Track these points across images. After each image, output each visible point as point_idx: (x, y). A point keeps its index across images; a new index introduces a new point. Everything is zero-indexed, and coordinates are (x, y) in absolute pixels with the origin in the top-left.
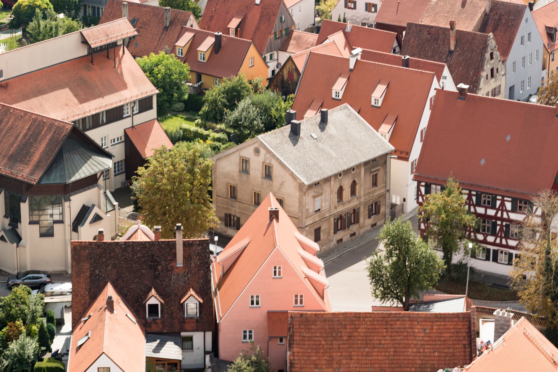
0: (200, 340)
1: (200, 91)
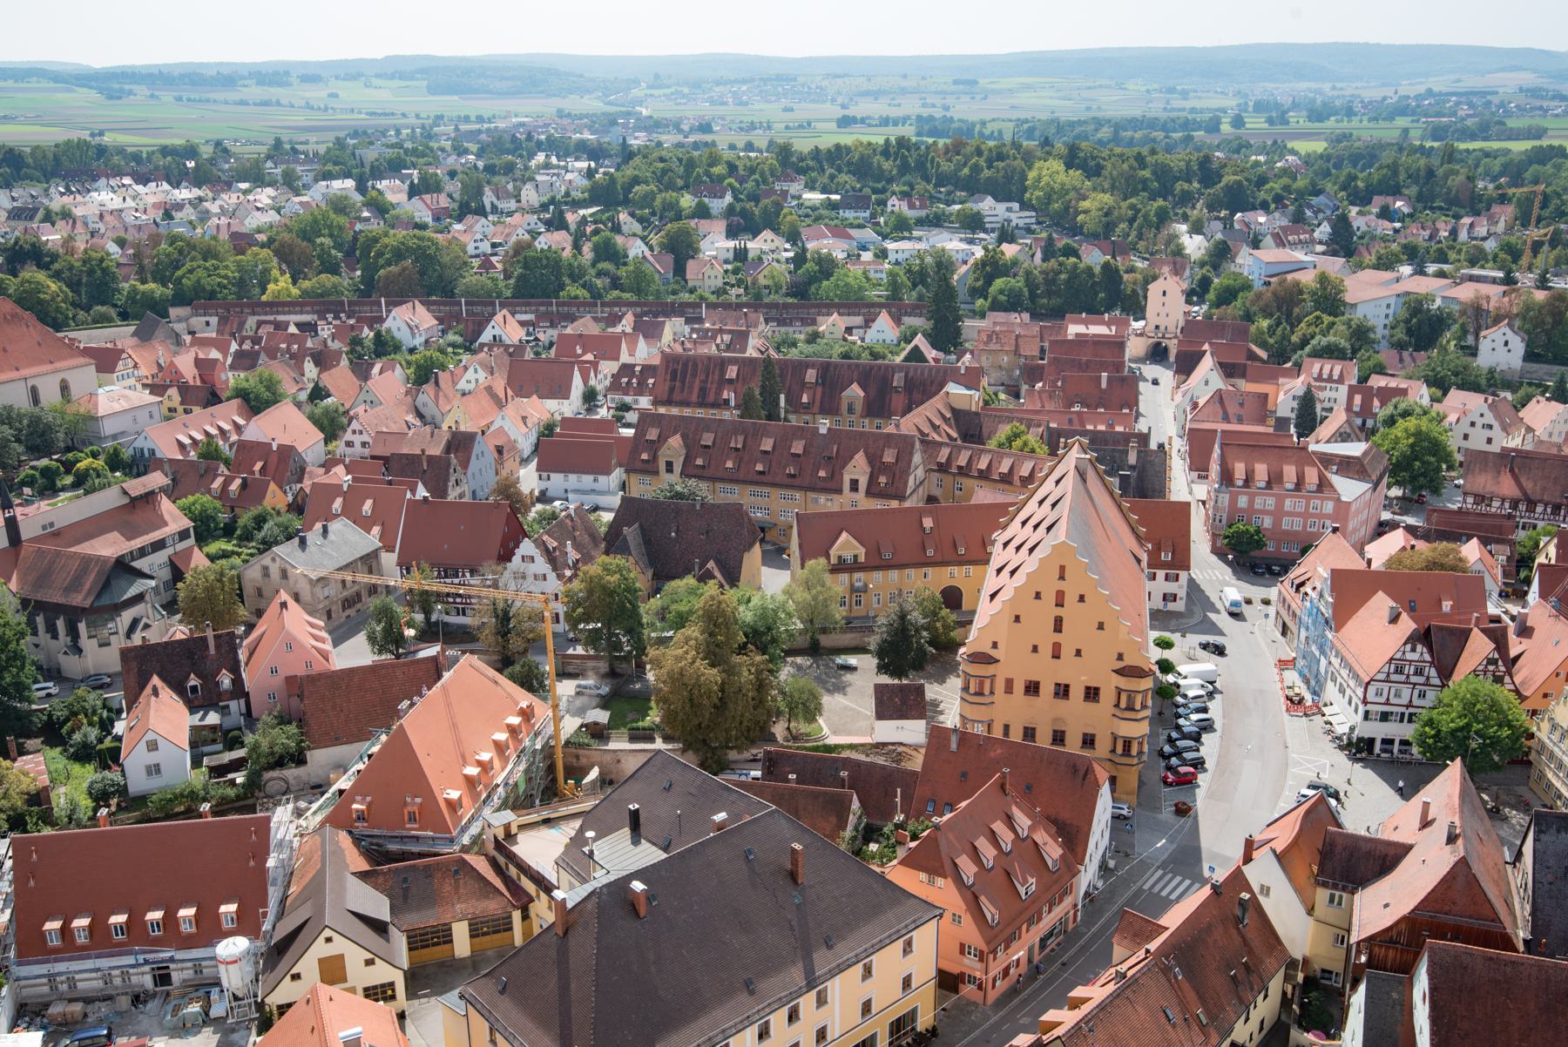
0: (235, 706)
1: (234, 520)
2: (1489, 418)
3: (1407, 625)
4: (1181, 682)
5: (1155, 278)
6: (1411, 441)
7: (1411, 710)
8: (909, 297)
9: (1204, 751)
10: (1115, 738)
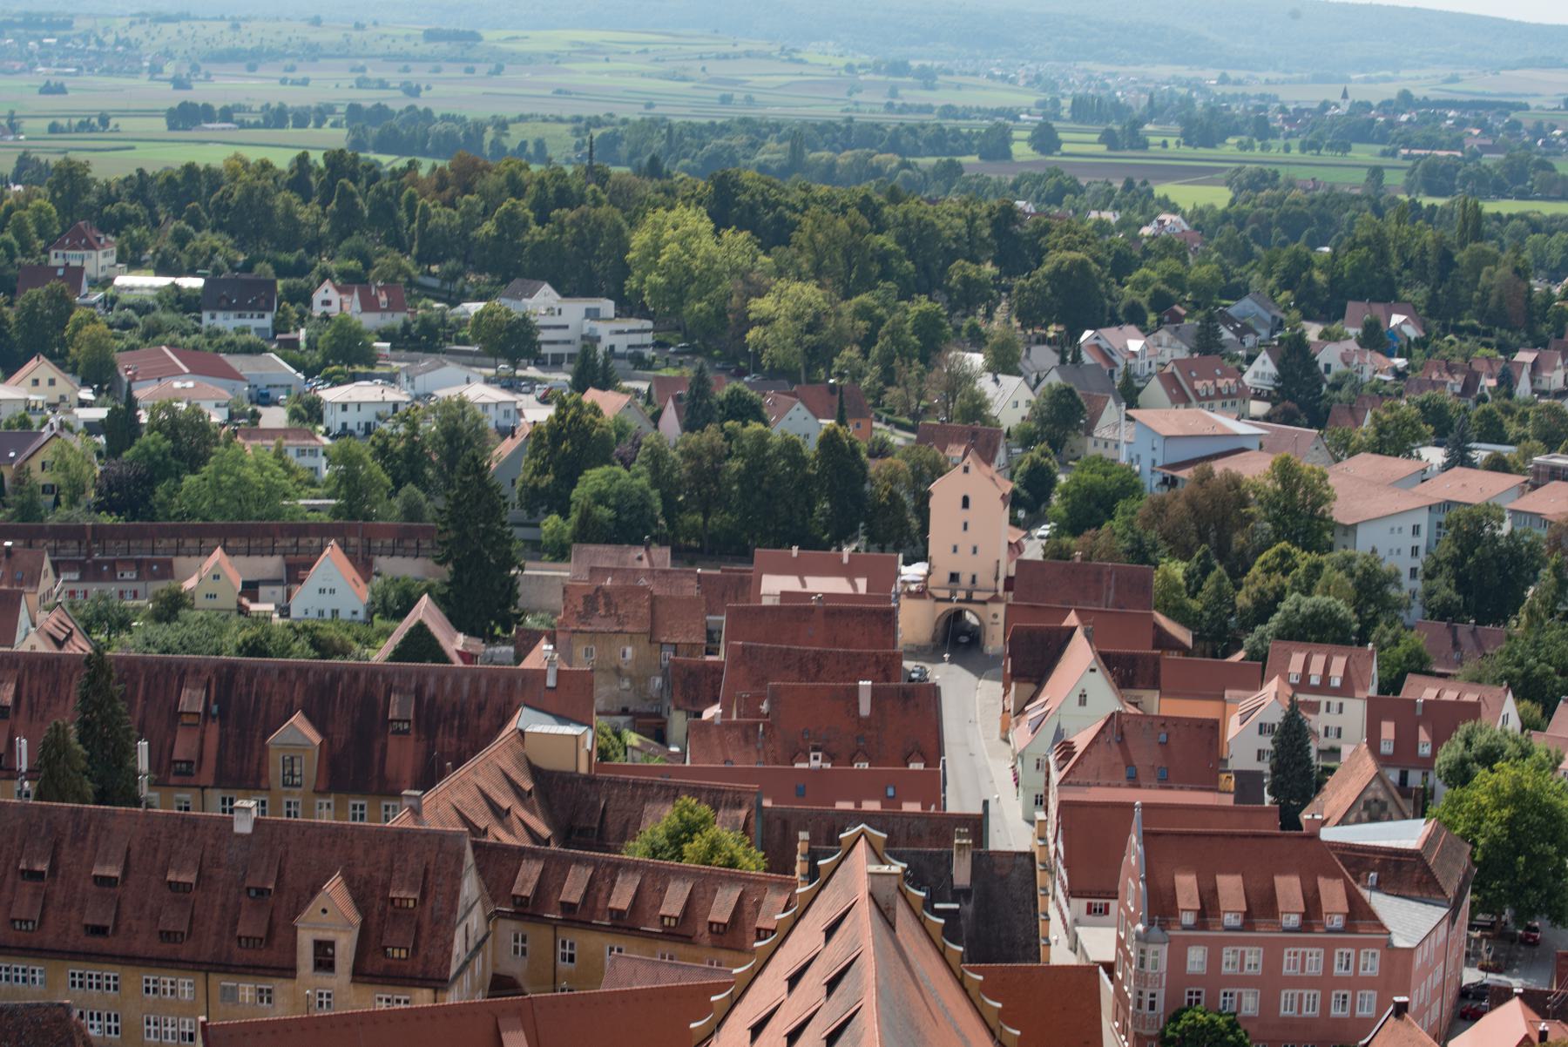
5: (938, 470)
6: (1506, 813)
8: (388, 511)
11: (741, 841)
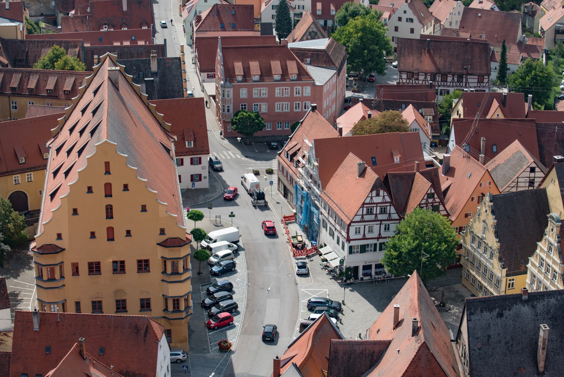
2: (410, 14)
3: (372, 176)
4: (212, 245)
6: (359, 35)
7: (381, 241)
9: (236, 298)
10: (166, 299)
11: (77, 60)
